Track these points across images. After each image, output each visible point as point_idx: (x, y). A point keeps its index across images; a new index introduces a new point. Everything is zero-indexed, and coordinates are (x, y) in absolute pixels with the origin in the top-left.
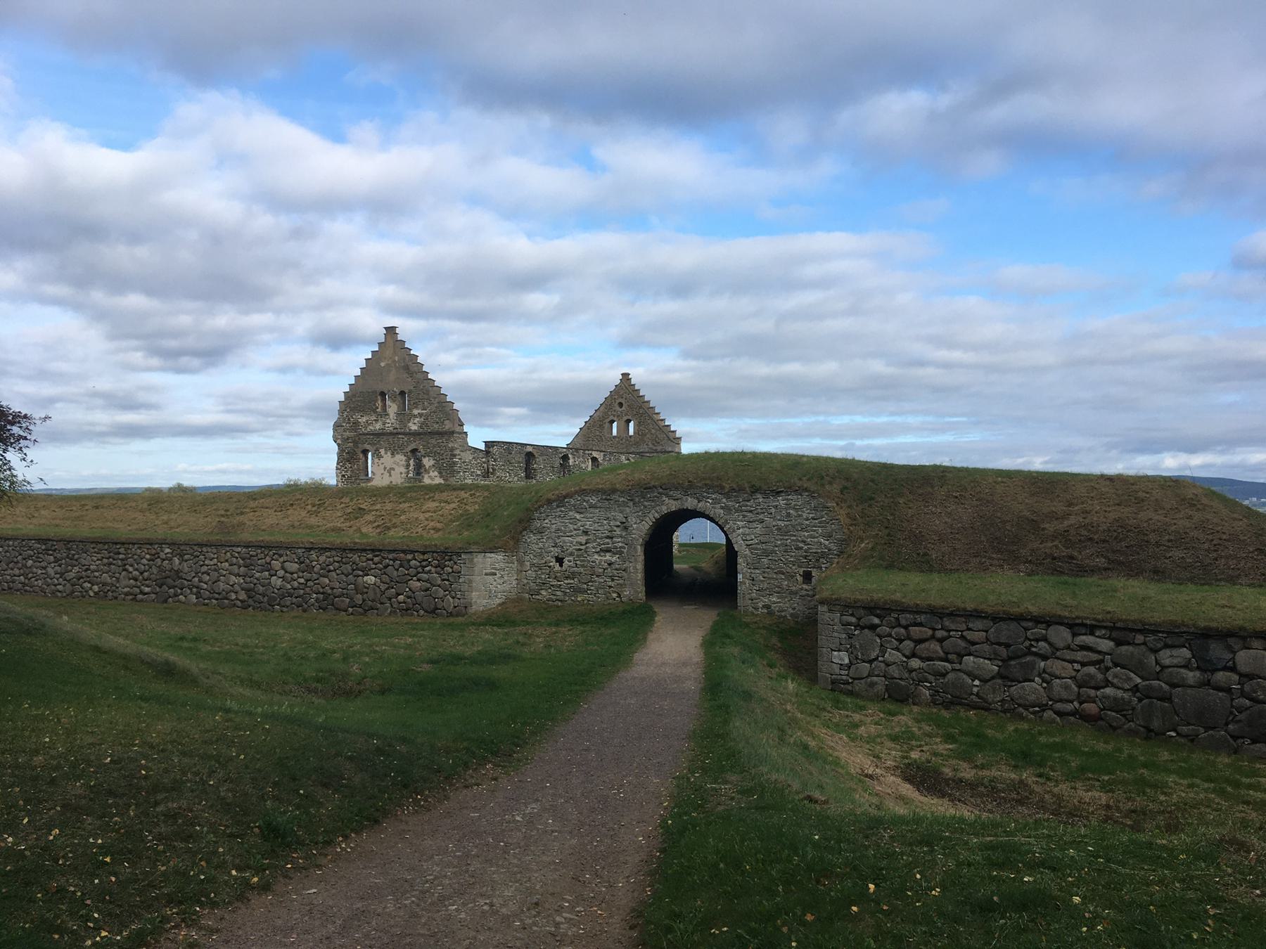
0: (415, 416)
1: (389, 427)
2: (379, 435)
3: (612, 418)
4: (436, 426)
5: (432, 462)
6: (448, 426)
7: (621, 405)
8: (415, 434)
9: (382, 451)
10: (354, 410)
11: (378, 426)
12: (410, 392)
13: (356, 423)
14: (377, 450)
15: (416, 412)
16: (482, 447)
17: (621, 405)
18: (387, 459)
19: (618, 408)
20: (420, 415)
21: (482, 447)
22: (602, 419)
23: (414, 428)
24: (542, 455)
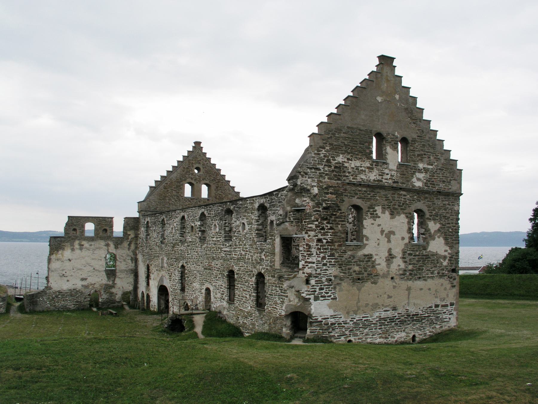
0: (420, 171)
1: (387, 180)
2: (375, 187)
4: (442, 185)
5: (438, 226)
6: (453, 188)
7: (198, 169)
8: (419, 192)
9: (379, 209)
10: (336, 149)
11: (373, 176)
12: (414, 141)
13: (340, 168)
14: (371, 207)
15: (421, 166)
18: (385, 219)
20: (426, 170)
23: (418, 184)
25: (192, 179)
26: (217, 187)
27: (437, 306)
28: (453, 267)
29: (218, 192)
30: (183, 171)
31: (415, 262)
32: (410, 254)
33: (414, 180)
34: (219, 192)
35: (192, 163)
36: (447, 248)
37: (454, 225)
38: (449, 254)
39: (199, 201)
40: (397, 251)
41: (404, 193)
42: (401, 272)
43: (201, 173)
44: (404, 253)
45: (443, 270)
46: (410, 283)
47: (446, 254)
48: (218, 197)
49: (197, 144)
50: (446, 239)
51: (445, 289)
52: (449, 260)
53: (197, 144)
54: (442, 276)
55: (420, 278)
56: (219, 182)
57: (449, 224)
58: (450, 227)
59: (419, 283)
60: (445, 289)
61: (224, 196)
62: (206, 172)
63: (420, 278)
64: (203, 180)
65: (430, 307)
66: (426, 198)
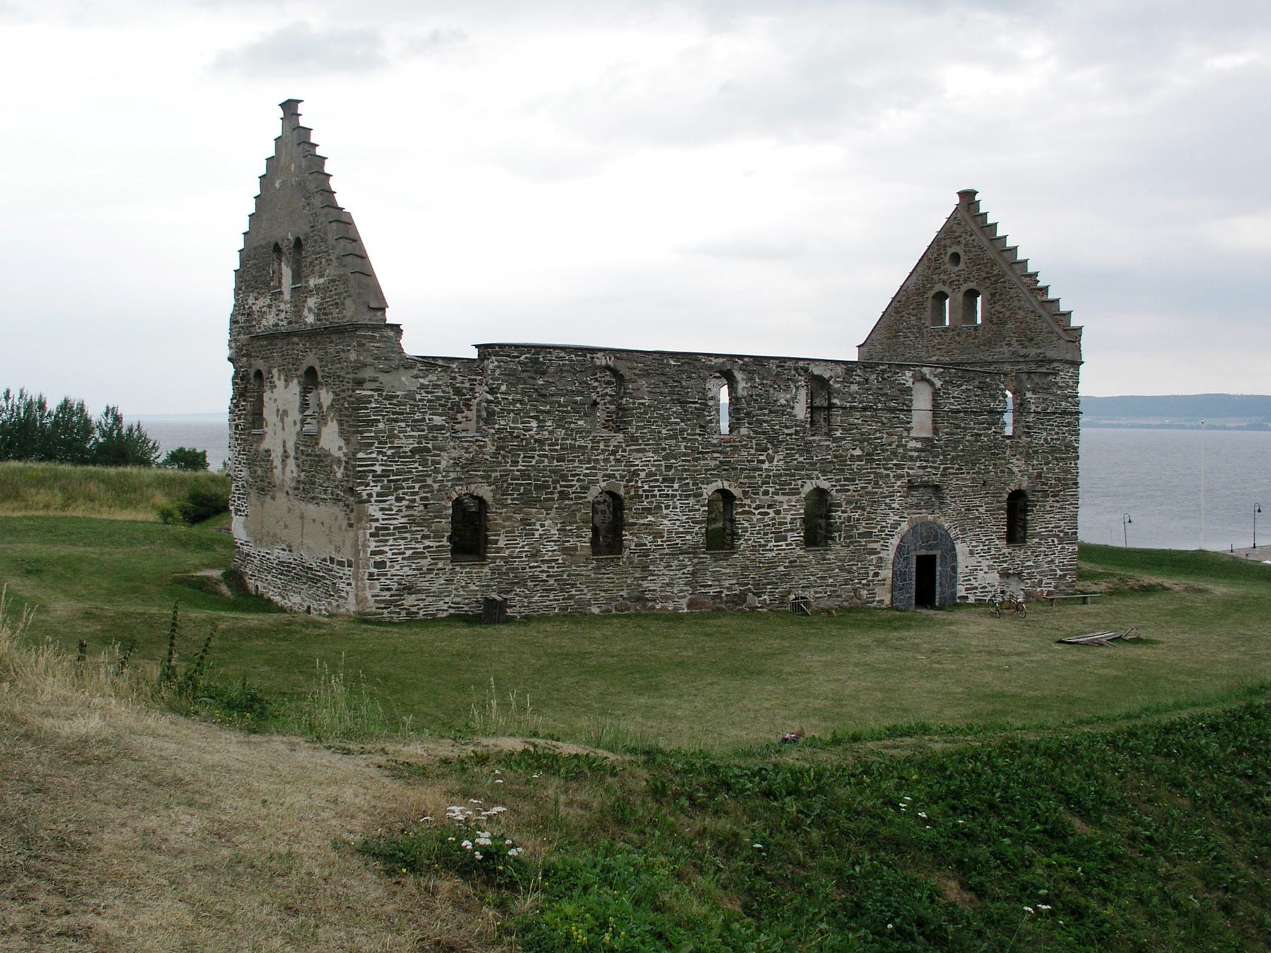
0: (310, 292)
3: (939, 287)
16: (474, 354)
17: (956, 258)
19: (949, 267)
20: (317, 287)
21: (474, 354)
22: (920, 291)
24: (646, 374)
25: (944, 282)
26: (993, 295)
27: (332, 560)
28: (350, 485)
29: (998, 307)
30: (929, 268)
31: (306, 467)
32: (302, 452)
33: (306, 312)
34: (998, 307)
35: (945, 246)
36: (342, 443)
37: (350, 393)
38: (345, 455)
39: (959, 335)
40: (290, 446)
41: (296, 339)
42: (294, 484)
43: (962, 266)
44: (297, 448)
45: (337, 487)
46: (303, 504)
47: (340, 454)
48: (995, 320)
49: (968, 198)
50: (340, 424)
51: (340, 528)
52: (346, 468)
53: (968, 198)
54: (336, 500)
55: (313, 498)
56: (996, 282)
57: (343, 391)
58: (344, 398)
59: (311, 509)
60: (340, 528)
61: (1008, 314)
62: (973, 261)
63: (313, 498)
64: (965, 281)
65: (325, 560)
66: (318, 343)
